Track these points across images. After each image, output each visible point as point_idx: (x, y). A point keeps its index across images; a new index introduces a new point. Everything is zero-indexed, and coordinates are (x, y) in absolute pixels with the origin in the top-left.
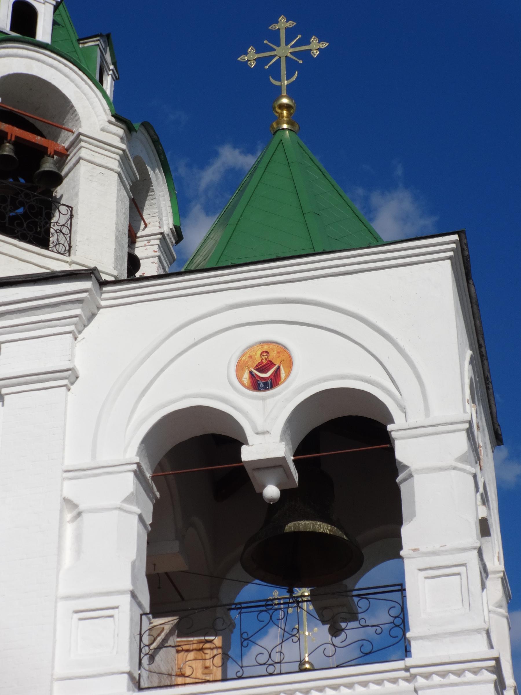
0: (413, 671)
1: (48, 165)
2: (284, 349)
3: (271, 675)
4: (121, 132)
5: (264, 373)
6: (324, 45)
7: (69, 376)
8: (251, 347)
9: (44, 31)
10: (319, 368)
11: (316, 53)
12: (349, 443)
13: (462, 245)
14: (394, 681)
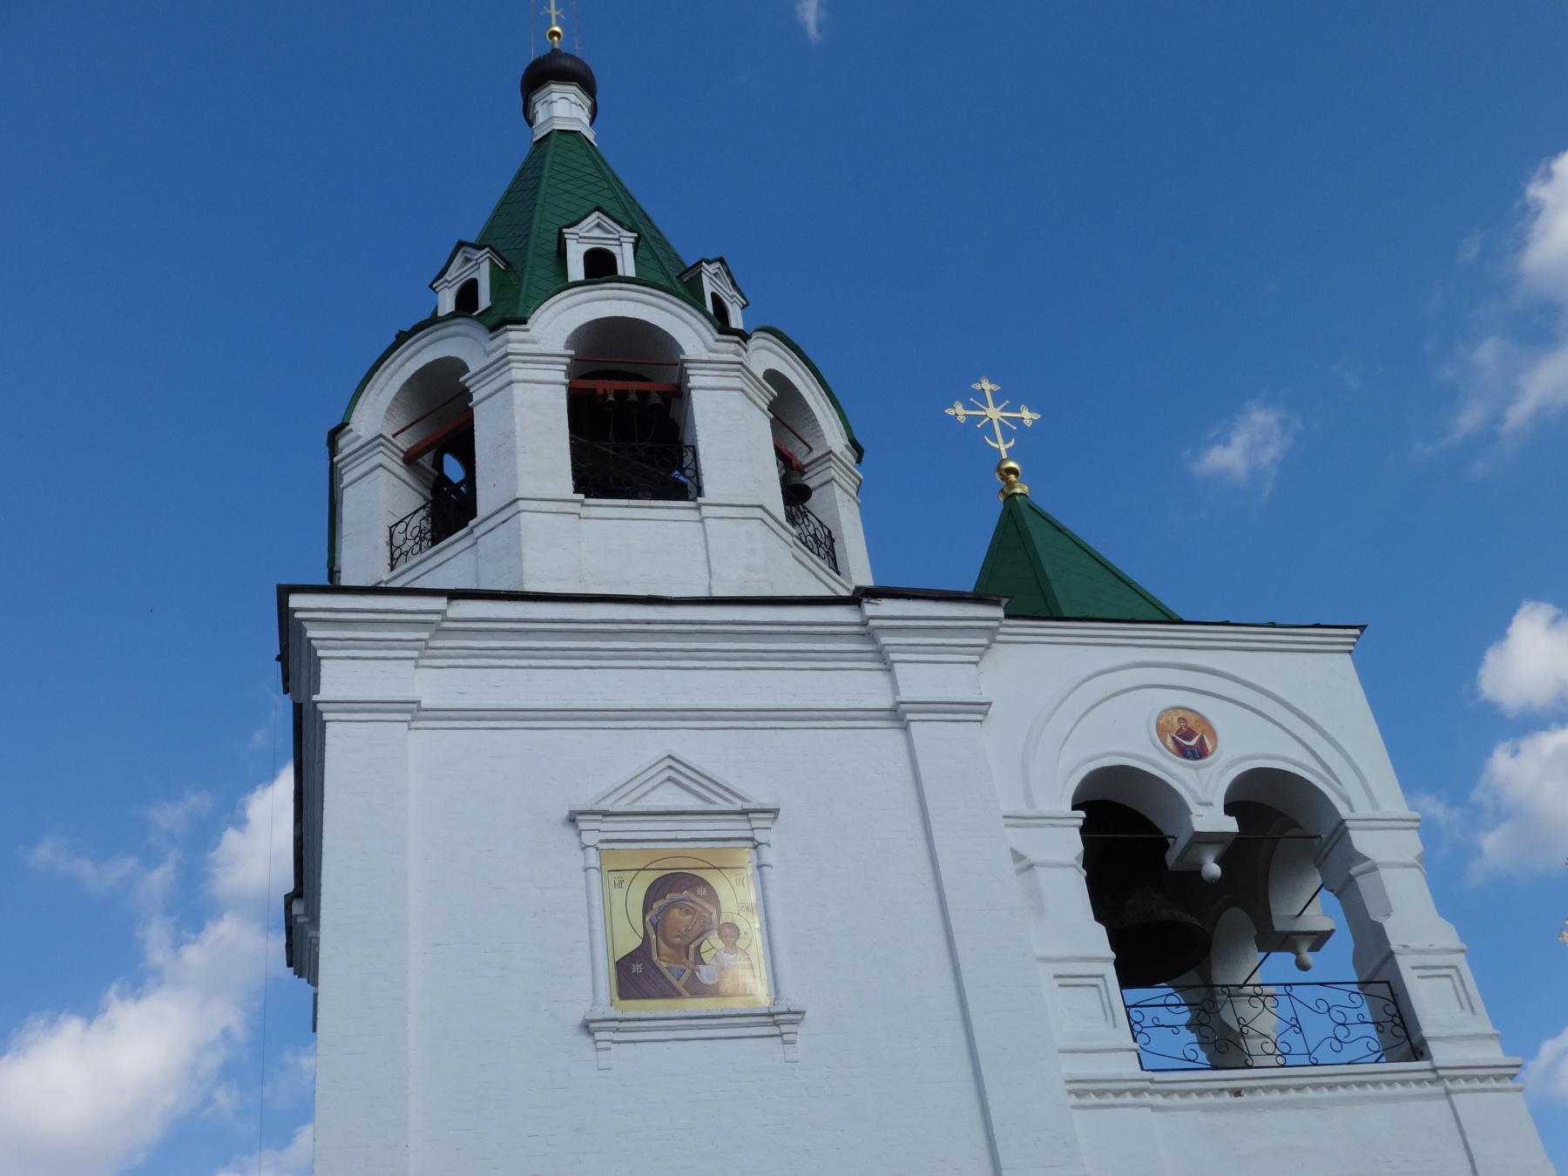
0: (1441, 1072)
2: (1202, 720)
5: (1190, 742)
6: (1036, 416)
7: (979, 709)
8: (1166, 711)
10: (1243, 746)
11: (1028, 423)
14: (1419, 1082)
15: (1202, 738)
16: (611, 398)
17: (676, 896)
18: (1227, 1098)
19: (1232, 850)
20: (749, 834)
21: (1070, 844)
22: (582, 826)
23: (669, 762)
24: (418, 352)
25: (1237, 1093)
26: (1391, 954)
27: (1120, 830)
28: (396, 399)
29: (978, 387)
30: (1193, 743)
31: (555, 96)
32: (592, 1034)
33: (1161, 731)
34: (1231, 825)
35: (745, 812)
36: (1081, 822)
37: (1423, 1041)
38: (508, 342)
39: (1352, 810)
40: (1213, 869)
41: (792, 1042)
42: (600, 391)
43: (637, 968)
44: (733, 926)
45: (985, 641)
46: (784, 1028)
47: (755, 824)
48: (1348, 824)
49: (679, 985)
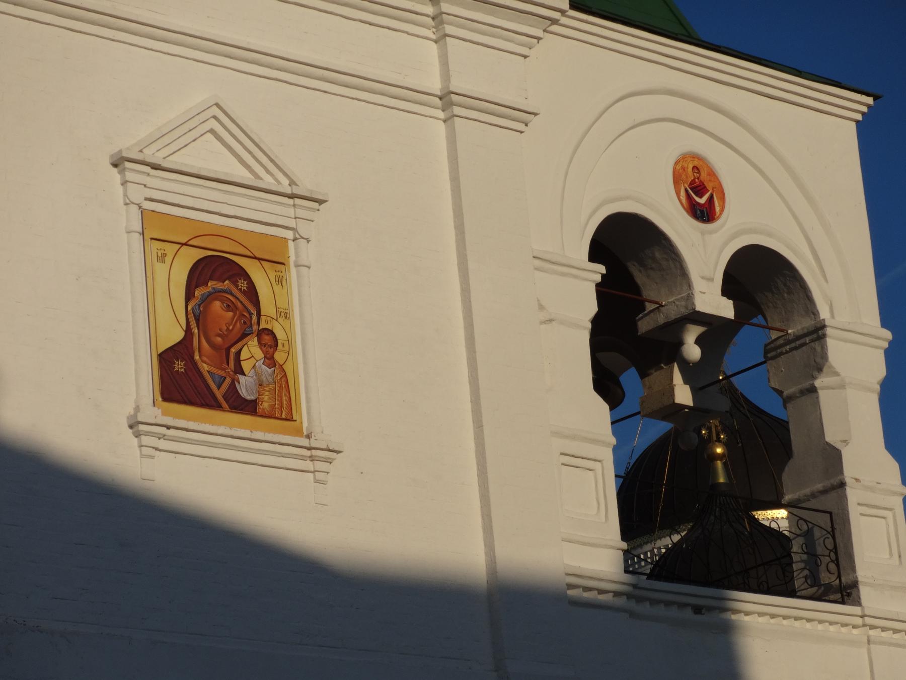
5: (701, 198)
7: (520, 116)
15: (711, 197)
17: (218, 285)
18: (688, 613)
20: (292, 223)
22: (129, 176)
23: (216, 111)
26: (842, 485)
30: (702, 201)
32: (137, 435)
33: (677, 180)
34: (726, 309)
35: (292, 196)
36: (598, 278)
37: (855, 585)
39: (833, 316)
41: (323, 483)
43: (179, 366)
44: (271, 333)
45: (539, 33)
46: (320, 465)
47: (301, 213)
48: (829, 331)
49: (219, 394)
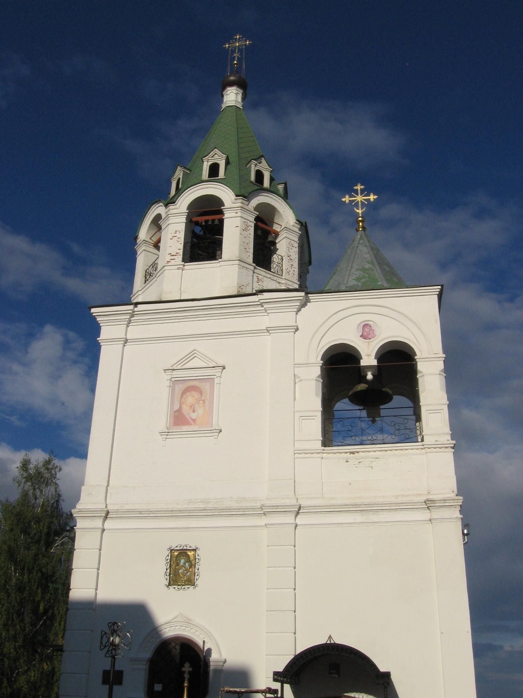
1: (270, 239)
3: (373, 444)
4: (299, 226)
9: (266, 183)
10: (389, 332)
12: (398, 360)
13: (442, 290)
16: (203, 224)
19: (379, 370)
21: (317, 371)
24: (154, 211)
25: (353, 453)
27: (339, 365)
28: (149, 227)
29: (356, 188)
31: (229, 92)
35: (214, 367)
36: (321, 365)
38: (170, 210)
40: (370, 376)
42: (200, 221)
